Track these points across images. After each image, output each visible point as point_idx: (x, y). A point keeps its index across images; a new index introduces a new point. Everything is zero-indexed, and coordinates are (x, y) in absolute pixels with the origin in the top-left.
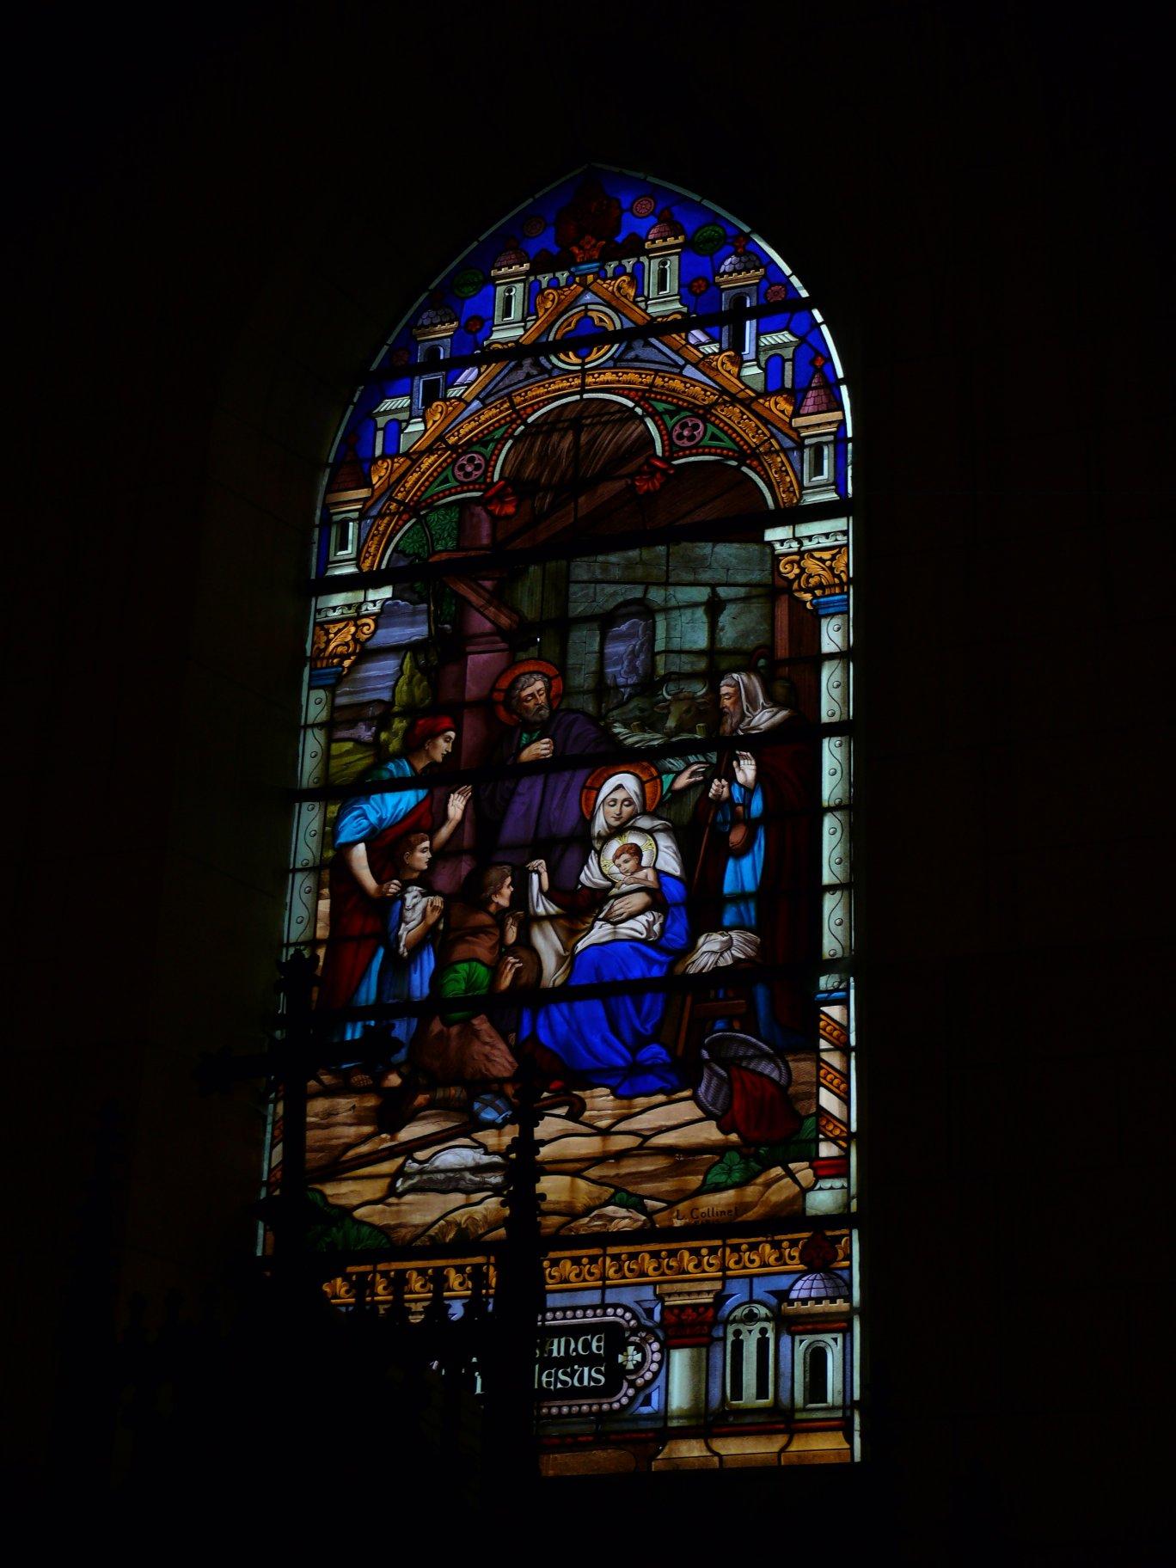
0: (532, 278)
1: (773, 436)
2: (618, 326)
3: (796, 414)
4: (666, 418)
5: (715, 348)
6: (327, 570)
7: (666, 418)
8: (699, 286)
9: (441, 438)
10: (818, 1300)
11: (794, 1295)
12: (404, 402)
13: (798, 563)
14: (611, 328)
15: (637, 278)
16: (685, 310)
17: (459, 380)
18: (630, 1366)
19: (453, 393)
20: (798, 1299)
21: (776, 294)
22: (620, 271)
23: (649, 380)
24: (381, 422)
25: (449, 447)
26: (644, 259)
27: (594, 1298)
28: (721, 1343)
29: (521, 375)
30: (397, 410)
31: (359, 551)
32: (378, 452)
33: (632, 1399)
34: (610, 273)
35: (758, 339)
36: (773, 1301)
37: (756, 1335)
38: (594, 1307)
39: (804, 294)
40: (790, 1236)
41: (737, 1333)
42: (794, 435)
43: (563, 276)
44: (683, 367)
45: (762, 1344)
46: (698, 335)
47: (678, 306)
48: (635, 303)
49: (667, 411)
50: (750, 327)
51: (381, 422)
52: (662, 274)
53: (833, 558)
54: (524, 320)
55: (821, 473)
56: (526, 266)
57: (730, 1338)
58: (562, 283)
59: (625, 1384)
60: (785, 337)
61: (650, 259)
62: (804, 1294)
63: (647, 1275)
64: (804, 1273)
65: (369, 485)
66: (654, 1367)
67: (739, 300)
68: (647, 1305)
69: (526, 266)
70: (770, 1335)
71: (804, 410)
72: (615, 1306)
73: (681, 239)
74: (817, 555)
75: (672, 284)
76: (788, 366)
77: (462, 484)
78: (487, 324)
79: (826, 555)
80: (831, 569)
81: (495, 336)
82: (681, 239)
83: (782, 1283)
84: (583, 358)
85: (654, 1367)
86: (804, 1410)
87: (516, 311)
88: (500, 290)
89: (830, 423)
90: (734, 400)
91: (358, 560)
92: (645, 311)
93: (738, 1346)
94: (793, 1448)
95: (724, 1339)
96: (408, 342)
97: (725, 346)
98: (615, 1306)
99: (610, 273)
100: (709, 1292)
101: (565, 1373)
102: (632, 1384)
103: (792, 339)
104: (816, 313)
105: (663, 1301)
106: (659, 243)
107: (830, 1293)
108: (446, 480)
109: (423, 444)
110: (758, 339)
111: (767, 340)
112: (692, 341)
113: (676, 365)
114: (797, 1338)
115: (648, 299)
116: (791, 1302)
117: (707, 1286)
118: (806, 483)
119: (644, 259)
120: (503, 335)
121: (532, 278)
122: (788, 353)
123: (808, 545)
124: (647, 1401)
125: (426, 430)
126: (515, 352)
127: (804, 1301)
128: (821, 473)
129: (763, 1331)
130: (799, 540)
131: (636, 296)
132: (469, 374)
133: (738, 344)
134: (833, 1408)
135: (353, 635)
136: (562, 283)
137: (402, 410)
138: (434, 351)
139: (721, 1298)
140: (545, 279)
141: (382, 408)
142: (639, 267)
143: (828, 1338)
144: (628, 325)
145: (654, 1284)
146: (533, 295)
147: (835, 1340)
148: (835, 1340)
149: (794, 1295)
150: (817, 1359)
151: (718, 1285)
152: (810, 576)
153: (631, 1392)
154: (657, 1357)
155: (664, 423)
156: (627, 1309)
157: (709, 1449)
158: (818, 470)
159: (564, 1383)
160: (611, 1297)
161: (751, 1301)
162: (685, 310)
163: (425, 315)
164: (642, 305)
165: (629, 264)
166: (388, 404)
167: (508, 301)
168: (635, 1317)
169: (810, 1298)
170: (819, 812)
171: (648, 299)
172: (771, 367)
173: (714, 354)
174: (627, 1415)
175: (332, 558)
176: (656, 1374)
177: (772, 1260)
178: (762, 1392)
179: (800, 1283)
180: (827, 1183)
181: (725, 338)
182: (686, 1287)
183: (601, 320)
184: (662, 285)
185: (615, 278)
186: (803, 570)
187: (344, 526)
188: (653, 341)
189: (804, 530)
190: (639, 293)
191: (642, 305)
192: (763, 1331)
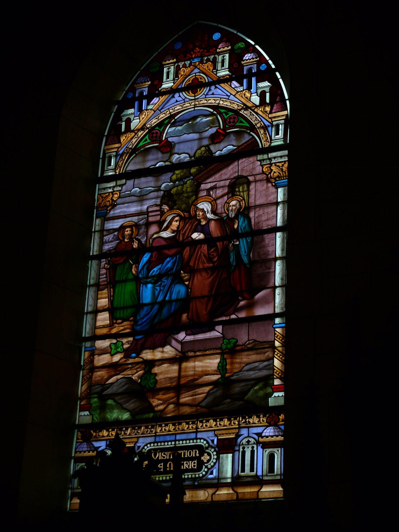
0: (177, 64)
1: (262, 120)
2: (207, 81)
3: (271, 112)
4: (224, 115)
5: (241, 89)
6: (104, 173)
7: (224, 115)
8: (235, 66)
9: (145, 125)
10: (272, 436)
11: (263, 434)
12: (131, 111)
13: (270, 167)
14: (204, 82)
15: (214, 62)
17: (152, 103)
18: (205, 461)
19: (150, 107)
20: (265, 436)
21: (263, 67)
23: (218, 102)
24: (124, 119)
25: (148, 128)
26: (217, 56)
27: (193, 436)
28: (238, 452)
29: (173, 100)
31: (116, 167)
32: (123, 130)
33: (207, 472)
35: (257, 85)
37: (250, 449)
38: (193, 439)
39: (273, 66)
41: (244, 448)
42: (270, 120)
43: (188, 63)
44: (229, 96)
45: (252, 452)
46: (235, 83)
47: (228, 73)
48: (213, 72)
49: (225, 113)
50: (254, 80)
51: (124, 119)
53: (283, 165)
54: (174, 80)
55: (278, 135)
56: (175, 60)
57: (241, 450)
58: (188, 66)
59: (204, 467)
60: (267, 84)
61: (219, 55)
62: (267, 434)
64: (267, 426)
65: (119, 142)
66: (214, 461)
67: (250, 70)
68: (211, 439)
69: (175, 60)
70: (255, 449)
71: (273, 111)
72: (200, 439)
73: (230, 48)
74: (278, 164)
75: (226, 64)
78: (161, 82)
79: (280, 165)
80: (282, 169)
81: (163, 86)
83: (259, 430)
85: (214, 461)
86: (267, 476)
87: (171, 77)
88: (165, 70)
89: (283, 116)
90: (247, 108)
91: (115, 169)
92: (216, 75)
93: (244, 453)
94: (262, 490)
95: (239, 450)
96: (133, 89)
97: (245, 88)
98: (200, 439)
100: (233, 433)
102: (206, 467)
103: (270, 84)
104: (278, 74)
105: (218, 437)
106: (222, 50)
107: (277, 434)
108: (146, 140)
109: (139, 126)
110: (257, 85)
111: (261, 85)
112: (233, 86)
113: (227, 95)
114: (265, 450)
115: (217, 70)
116: (262, 437)
117: (234, 431)
118: (273, 138)
119: (217, 56)
120: (167, 85)
121: (177, 64)
122: (267, 90)
123: (273, 161)
124: (212, 473)
126: (172, 92)
127: (267, 437)
128: (278, 135)
129: (253, 447)
130: (270, 159)
131: (213, 69)
132: (155, 100)
133: (249, 88)
134: (277, 475)
135: (112, 198)
136: (188, 66)
138: (142, 93)
139: (238, 435)
140: (181, 64)
141: (124, 113)
142: (215, 59)
143: (275, 450)
144: (210, 80)
145: (214, 430)
146: (177, 70)
147: (278, 451)
148: (278, 451)
149: (263, 434)
150: (271, 457)
151: (237, 431)
152: (275, 172)
153: (206, 470)
154: (215, 457)
155: (224, 117)
156: (205, 440)
157: (233, 490)
158: (277, 133)
160: (199, 435)
161: (249, 436)
164: (215, 73)
167: (168, 73)
168: (208, 442)
169: (270, 436)
171: (217, 70)
172: (262, 96)
173: (241, 91)
174: (204, 478)
175: (106, 169)
176: (215, 463)
178: (252, 470)
179: (266, 430)
180: (276, 394)
182: (227, 432)
183: (201, 79)
184: (223, 65)
185: (206, 63)
186: (272, 170)
187: (110, 158)
189: (271, 155)
190: (215, 67)
191: (215, 73)
192: (253, 447)
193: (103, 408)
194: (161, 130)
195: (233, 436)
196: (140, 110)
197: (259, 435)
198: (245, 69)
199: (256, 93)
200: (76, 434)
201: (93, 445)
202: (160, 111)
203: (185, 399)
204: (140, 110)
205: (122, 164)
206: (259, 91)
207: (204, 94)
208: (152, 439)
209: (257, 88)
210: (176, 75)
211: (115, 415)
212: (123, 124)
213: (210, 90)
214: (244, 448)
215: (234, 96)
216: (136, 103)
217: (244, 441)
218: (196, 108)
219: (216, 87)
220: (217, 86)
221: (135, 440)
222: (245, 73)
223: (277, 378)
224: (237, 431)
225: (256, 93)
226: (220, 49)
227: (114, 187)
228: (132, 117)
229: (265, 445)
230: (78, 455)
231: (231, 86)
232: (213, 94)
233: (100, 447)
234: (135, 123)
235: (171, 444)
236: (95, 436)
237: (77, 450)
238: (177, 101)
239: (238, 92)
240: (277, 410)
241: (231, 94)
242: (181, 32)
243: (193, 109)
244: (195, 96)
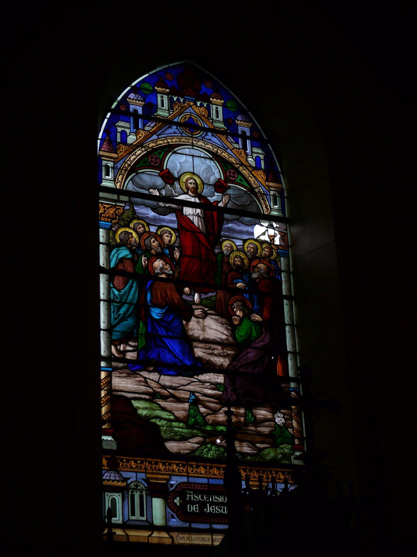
1: (260, 186)
5: (236, 146)
12: (128, 125)
14: (200, 125)
16: (226, 128)
19: (147, 128)
22: (202, 105)
24: (119, 129)
30: (124, 127)
34: (198, 105)
35: (252, 149)
40: (155, 460)
42: (267, 188)
46: (230, 139)
47: (223, 126)
50: (248, 142)
51: (119, 129)
52: (217, 112)
54: (169, 110)
60: (260, 151)
63: (161, 471)
69: (168, 90)
76: (262, 162)
77: (152, 166)
81: (159, 113)
82: (222, 101)
84: (192, 133)
87: (166, 106)
99: (198, 105)
101: (218, 508)
113: (224, 147)
122: (262, 157)
125: (137, 140)
133: (245, 148)
137: (127, 128)
144: (206, 126)
159: (218, 511)
162: (226, 128)
163: (131, 95)
165: (205, 105)
166: (120, 123)
167: (162, 101)
170: (285, 325)
172: (257, 160)
177: (204, 472)
181: (240, 143)
183: (197, 121)
188: (178, 128)
194: (161, 157)
196: (136, 126)
198: (240, 129)
199: (252, 155)
201: (121, 475)
202: (158, 136)
204: (136, 126)
205: (123, 178)
206: (254, 155)
207: (201, 136)
209: (252, 152)
210: (171, 107)
212: (119, 135)
213: (206, 135)
214: (132, 492)
215: (231, 150)
216: (132, 119)
218: (194, 147)
219: (213, 135)
220: (214, 134)
222: (240, 133)
223: (297, 438)
225: (252, 155)
226: (213, 98)
227: (115, 201)
228: (128, 131)
231: (227, 139)
232: (210, 140)
233: (129, 479)
234: (131, 139)
235: (205, 487)
236: (122, 466)
237: (104, 478)
238: (175, 133)
239: (235, 148)
241: (228, 148)
242: (206, 71)
243: (191, 147)
244: (192, 135)
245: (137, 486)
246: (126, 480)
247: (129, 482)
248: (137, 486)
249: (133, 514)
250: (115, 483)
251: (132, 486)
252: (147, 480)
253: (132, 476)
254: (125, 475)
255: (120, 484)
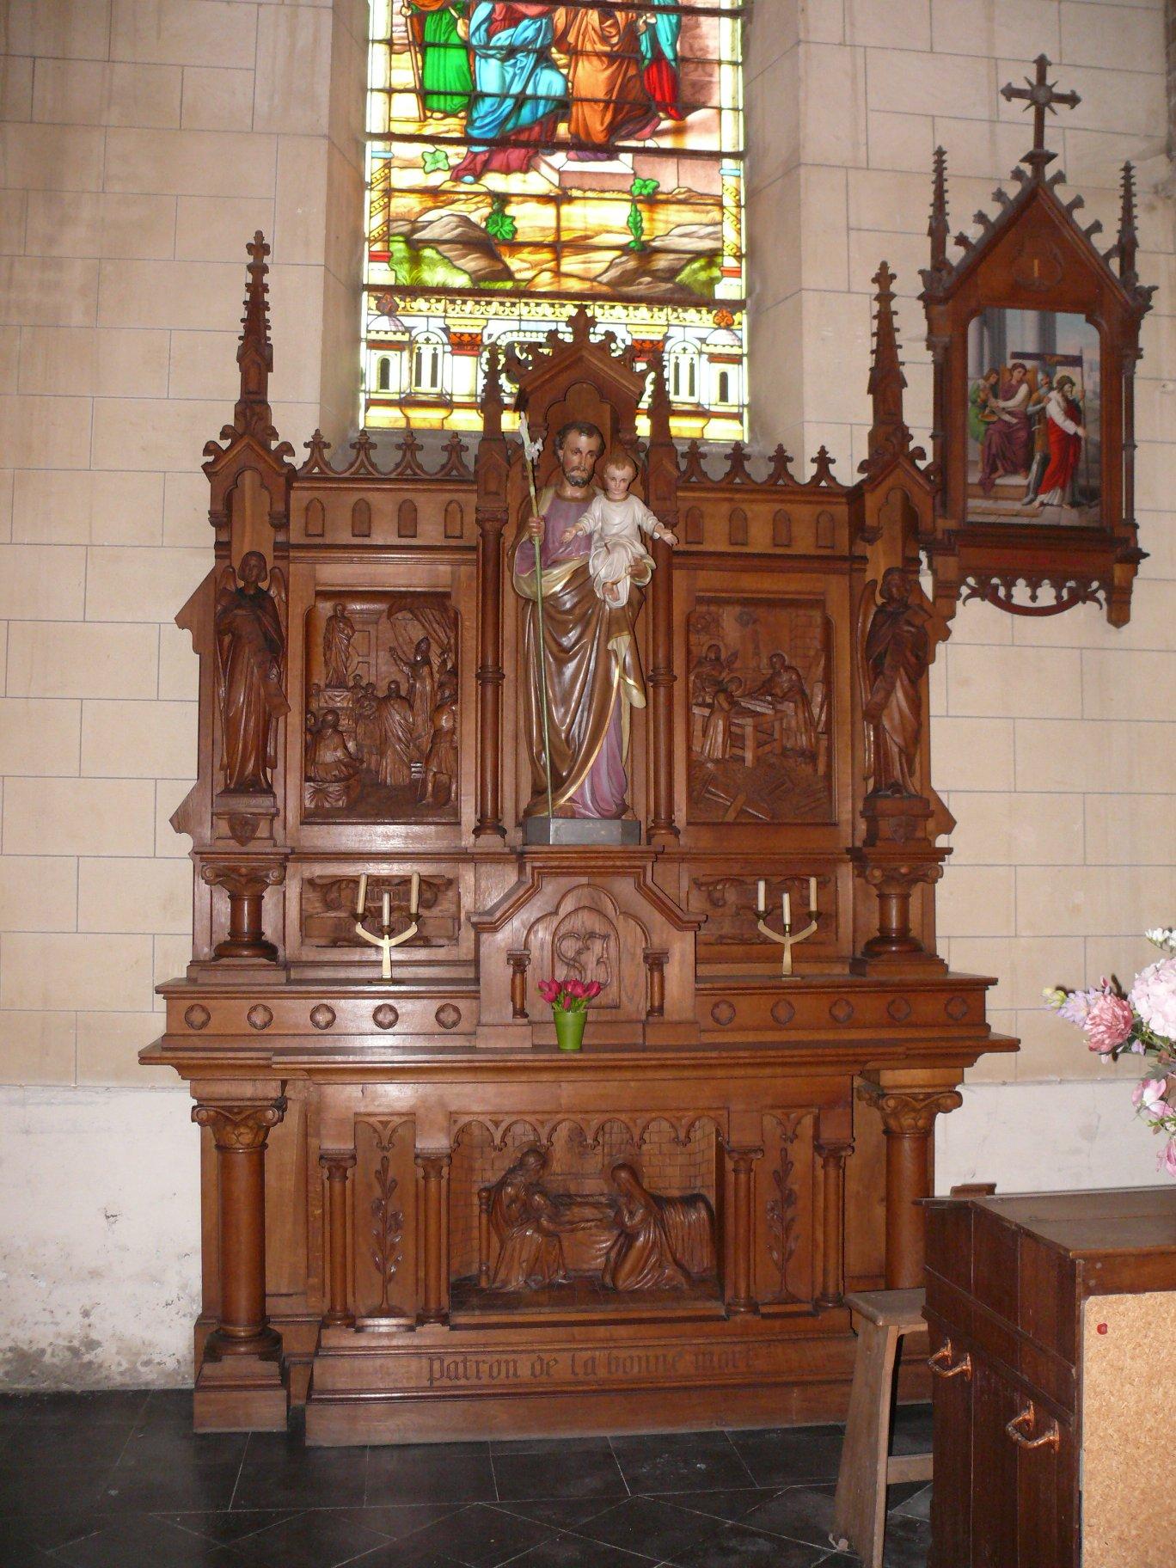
36: (698, 344)
83: (703, 333)
139: (667, 338)
151: (665, 329)
193: (415, 261)
195: (660, 337)
197: (703, 340)
200: (368, 302)
203: (570, 264)
208: (515, 325)
211: (436, 275)
217: (678, 348)
221: (484, 323)
224: (665, 329)
229: (714, 358)
230: (373, 336)
240: (736, 306)
245: (428, 340)
246: (408, 330)
247: (414, 333)
248: (428, 340)
249: (418, 383)
250: (390, 337)
251: (421, 339)
252: (446, 330)
253: (419, 324)
254: (407, 322)
255: (399, 337)
